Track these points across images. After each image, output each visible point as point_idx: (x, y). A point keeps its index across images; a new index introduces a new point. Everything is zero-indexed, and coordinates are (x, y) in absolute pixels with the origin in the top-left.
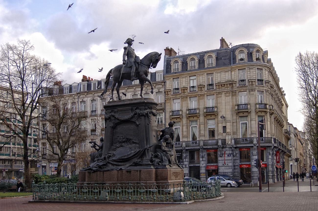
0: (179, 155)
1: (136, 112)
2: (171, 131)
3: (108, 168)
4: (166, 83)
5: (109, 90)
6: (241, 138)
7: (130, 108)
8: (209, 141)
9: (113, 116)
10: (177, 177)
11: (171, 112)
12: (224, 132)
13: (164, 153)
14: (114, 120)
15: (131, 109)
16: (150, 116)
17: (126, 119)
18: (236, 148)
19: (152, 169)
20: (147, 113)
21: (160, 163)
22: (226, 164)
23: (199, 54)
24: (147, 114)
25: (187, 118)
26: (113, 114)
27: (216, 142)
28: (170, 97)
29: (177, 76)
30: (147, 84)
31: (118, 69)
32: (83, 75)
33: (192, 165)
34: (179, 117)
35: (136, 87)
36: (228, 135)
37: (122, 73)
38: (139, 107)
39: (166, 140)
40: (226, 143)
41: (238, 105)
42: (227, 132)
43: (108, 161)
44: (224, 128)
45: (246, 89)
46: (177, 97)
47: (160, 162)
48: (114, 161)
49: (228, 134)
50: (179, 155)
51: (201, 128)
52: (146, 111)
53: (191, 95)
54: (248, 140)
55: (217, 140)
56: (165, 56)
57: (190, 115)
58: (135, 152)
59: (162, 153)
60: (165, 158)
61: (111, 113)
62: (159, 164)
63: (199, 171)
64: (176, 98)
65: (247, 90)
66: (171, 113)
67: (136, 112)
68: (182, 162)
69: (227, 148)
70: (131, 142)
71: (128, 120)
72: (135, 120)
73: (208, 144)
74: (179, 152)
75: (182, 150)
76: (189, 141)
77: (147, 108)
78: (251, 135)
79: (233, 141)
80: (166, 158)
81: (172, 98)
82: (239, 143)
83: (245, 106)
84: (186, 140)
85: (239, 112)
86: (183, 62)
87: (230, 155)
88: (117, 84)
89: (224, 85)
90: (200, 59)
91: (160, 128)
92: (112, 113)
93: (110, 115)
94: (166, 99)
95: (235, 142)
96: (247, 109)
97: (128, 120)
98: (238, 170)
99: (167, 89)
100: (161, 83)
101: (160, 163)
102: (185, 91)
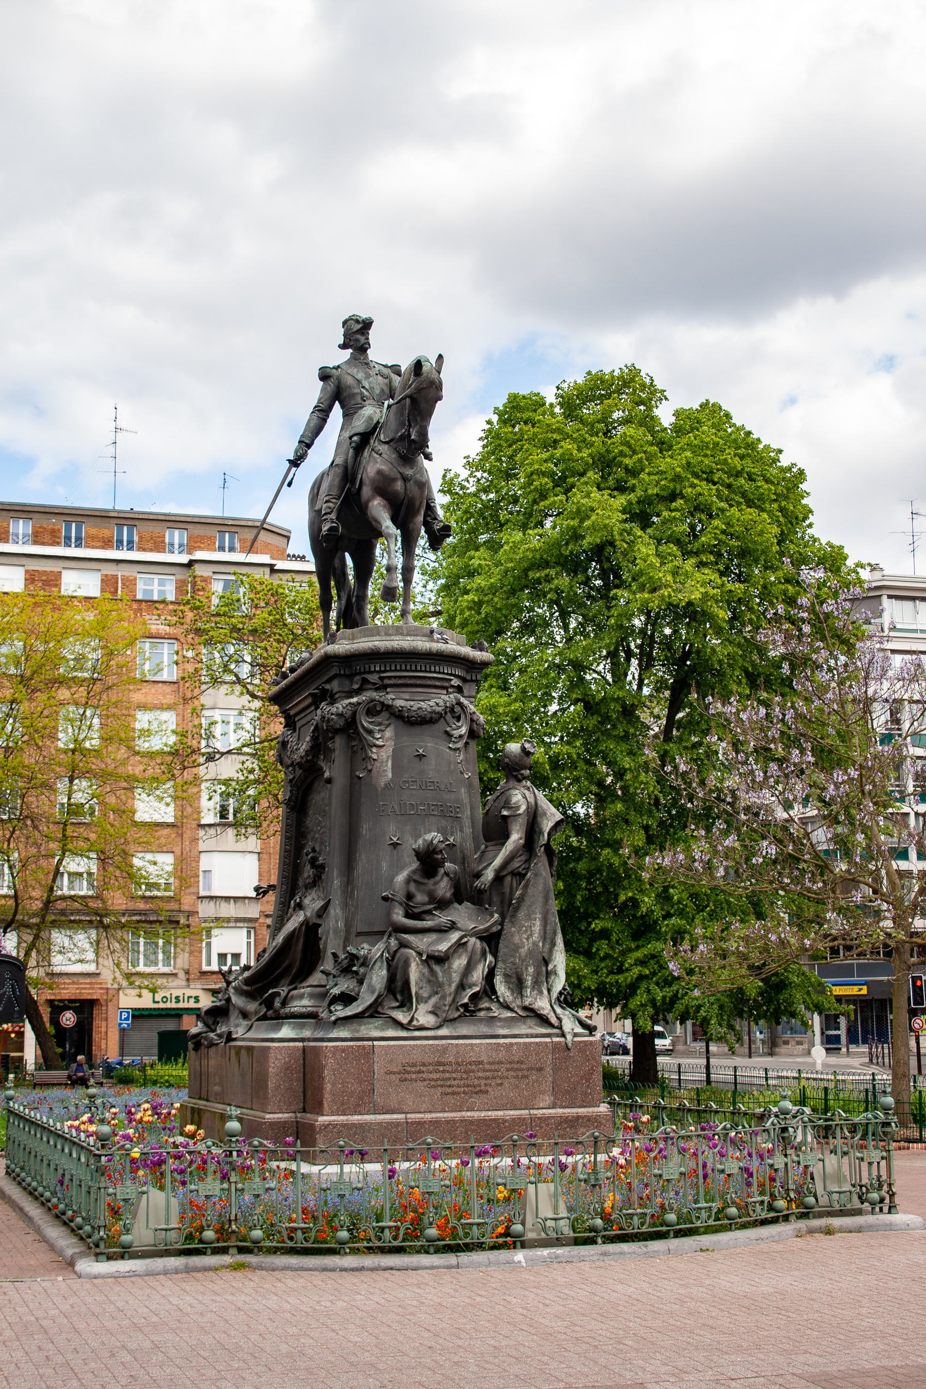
15: (310, 700)
16: (370, 732)
52: (341, 706)
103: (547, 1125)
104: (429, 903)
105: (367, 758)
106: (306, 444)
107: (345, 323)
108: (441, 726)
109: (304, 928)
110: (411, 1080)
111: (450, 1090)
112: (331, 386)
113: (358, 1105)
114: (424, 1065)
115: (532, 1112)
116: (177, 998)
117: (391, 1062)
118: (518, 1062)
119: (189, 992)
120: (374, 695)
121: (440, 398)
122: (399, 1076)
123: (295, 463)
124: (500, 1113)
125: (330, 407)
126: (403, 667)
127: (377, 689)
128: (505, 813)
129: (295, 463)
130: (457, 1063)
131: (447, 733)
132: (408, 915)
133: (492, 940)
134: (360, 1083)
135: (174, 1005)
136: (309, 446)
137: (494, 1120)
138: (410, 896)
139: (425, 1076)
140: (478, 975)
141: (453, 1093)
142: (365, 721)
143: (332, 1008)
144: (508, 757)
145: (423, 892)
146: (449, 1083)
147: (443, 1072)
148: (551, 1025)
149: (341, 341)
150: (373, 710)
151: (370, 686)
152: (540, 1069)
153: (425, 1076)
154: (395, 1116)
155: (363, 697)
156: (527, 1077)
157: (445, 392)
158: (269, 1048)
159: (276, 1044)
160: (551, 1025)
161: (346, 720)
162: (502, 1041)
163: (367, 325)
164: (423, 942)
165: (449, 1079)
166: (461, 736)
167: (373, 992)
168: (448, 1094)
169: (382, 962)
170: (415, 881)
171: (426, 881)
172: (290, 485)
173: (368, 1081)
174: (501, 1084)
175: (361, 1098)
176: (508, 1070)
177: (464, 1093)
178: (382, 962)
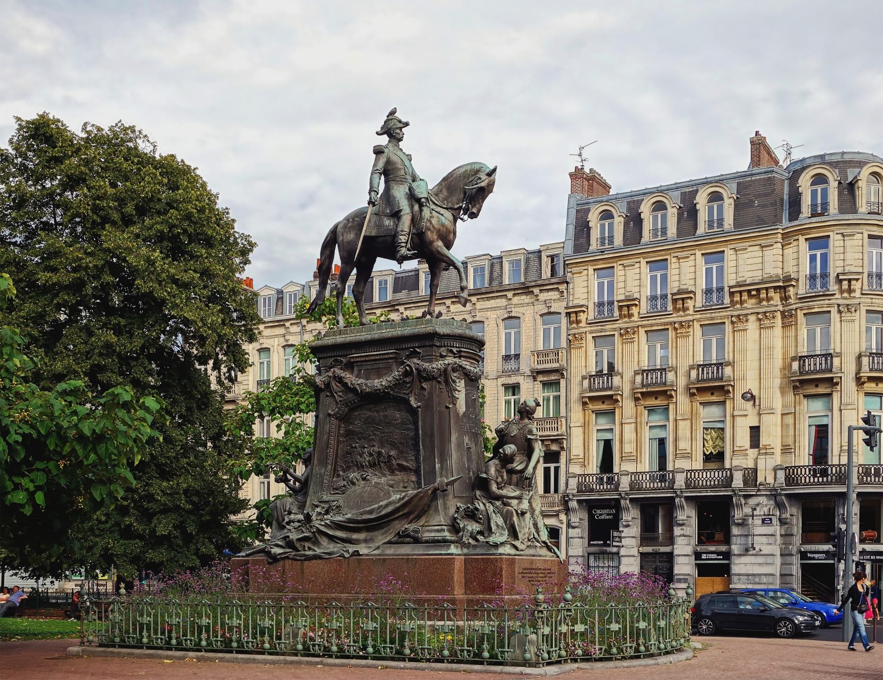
0: (608, 515)
1: (407, 368)
3: (318, 551)
4: (571, 286)
5: (396, 308)
6: (807, 466)
7: (392, 353)
8: (705, 473)
9: (340, 380)
11: (586, 378)
12: (752, 447)
13: (498, 503)
14: (340, 394)
18: (789, 496)
19: (452, 554)
21: (480, 537)
22: (754, 549)
23: (677, 188)
25: (637, 399)
26: (338, 371)
27: (726, 476)
28: (583, 330)
29: (609, 263)
30: (514, 289)
31: (356, 220)
33: (649, 549)
34: (611, 396)
35: (479, 297)
36: (763, 457)
37: (365, 237)
38: (418, 350)
39: (506, 460)
40: (757, 481)
41: (801, 357)
42: (761, 446)
43: (317, 526)
44: (755, 431)
45: (829, 305)
46: (605, 331)
47: (481, 533)
48: (338, 526)
49: (764, 451)
50: (611, 517)
51: (680, 433)
53: (652, 325)
54: (829, 473)
55: (728, 469)
56: (570, 195)
57: (644, 390)
58: (403, 498)
59: (490, 502)
60: (497, 520)
61: (332, 370)
62: (477, 540)
63: (671, 569)
64: (603, 334)
65: (832, 309)
66: (587, 380)
67: (407, 368)
68: (617, 539)
69: (760, 498)
71: (384, 391)
72: (408, 392)
73: (704, 484)
74: (611, 508)
75: (617, 501)
76: (640, 473)
77: (444, 354)
78: (840, 456)
79: (781, 475)
80: (500, 521)
81: (591, 332)
82: (799, 482)
83: (823, 362)
84: (630, 467)
85: (802, 382)
86: (627, 216)
87: (771, 519)
88: (355, 271)
89: (758, 290)
90: (682, 205)
91: (551, 429)
92: (336, 369)
93: (330, 377)
94: (570, 337)
95: (787, 478)
96: (831, 371)
97: (384, 392)
98: (796, 569)
99: (576, 302)
100: (555, 286)
101: (480, 537)
102: (635, 310)
120: (457, 360)
127: (455, 357)
128: (529, 437)
138: (497, 478)
148: (551, 552)
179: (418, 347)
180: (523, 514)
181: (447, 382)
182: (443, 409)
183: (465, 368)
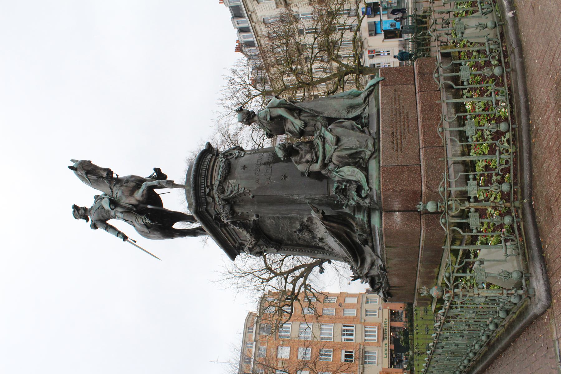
2: (265, 121)
10: (407, 113)
14: (261, 247)
15: (223, 229)
16: (232, 192)
17: (251, 235)
20: (223, 200)
24: (227, 201)
32: (235, 51)
38: (214, 217)
62: (366, 197)
70: (309, 223)
71: (251, 232)
97: (251, 232)
103: (424, 85)
104: (312, 153)
105: (244, 193)
106: (119, 233)
107: (76, 218)
108: (232, 161)
109: (325, 222)
110: (401, 147)
111: (406, 130)
112: (98, 224)
113: (416, 173)
114: (393, 142)
115: (417, 91)
116: (385, 350)
117: (391, 157)
118: (392, 100)
119: (384, 347)
120: (215, 188)
121: (90, 162)
122: (399, 153)
123: (125, 238)
124: (418, 105)
125: (107, 224)
126: (203, 176)
127: (213, 189)
128: (268, 118)
129: (125, 238)
130: (392, 127)
131: (236, 158)
132: (317, 162)
133: (330, 120)
134: (403, 171)
135: (387, 351)
136: (119, 233)
137: (422, 108)
138: (307, 161)
139: (399, 141)
140: (347, 123)
141: (408, 128)
142: (227, 194)
143: (363, 196)
144: (243, 120)
145: (305, 156)
146: (403, 130)
147: (397, 133)
148: (373, 90)
149: (85, 221)
150: (222, 191)
151: (212, 193)
152: (395, 90)
153: (399, 141)
154: (421, 154)
155: (216, 196)
156: (399, 96)
157: (87, 159)
158: (385, 229)
159: (383, 225)
160: (373, 90)
161: (226, 204)
162: (380, 107)
163: (75, 207)
164: (330, 148)
165: (401, 130)
166: (239, 153)
167: (354, 172)
168: (409, 130)
169: (340, 171)
170: (301, 159)
171: (300, 155)
172: (135, 242)
173: (402, 168)
174: (403, 106)
175: (412, 171)
176: (395, 104)
177: (408, 123)
178: (340, 171)
179: (212, 217)
180: (338, 140)
181: (234, 197)
182: (255, 199)
183: (220, 182)
